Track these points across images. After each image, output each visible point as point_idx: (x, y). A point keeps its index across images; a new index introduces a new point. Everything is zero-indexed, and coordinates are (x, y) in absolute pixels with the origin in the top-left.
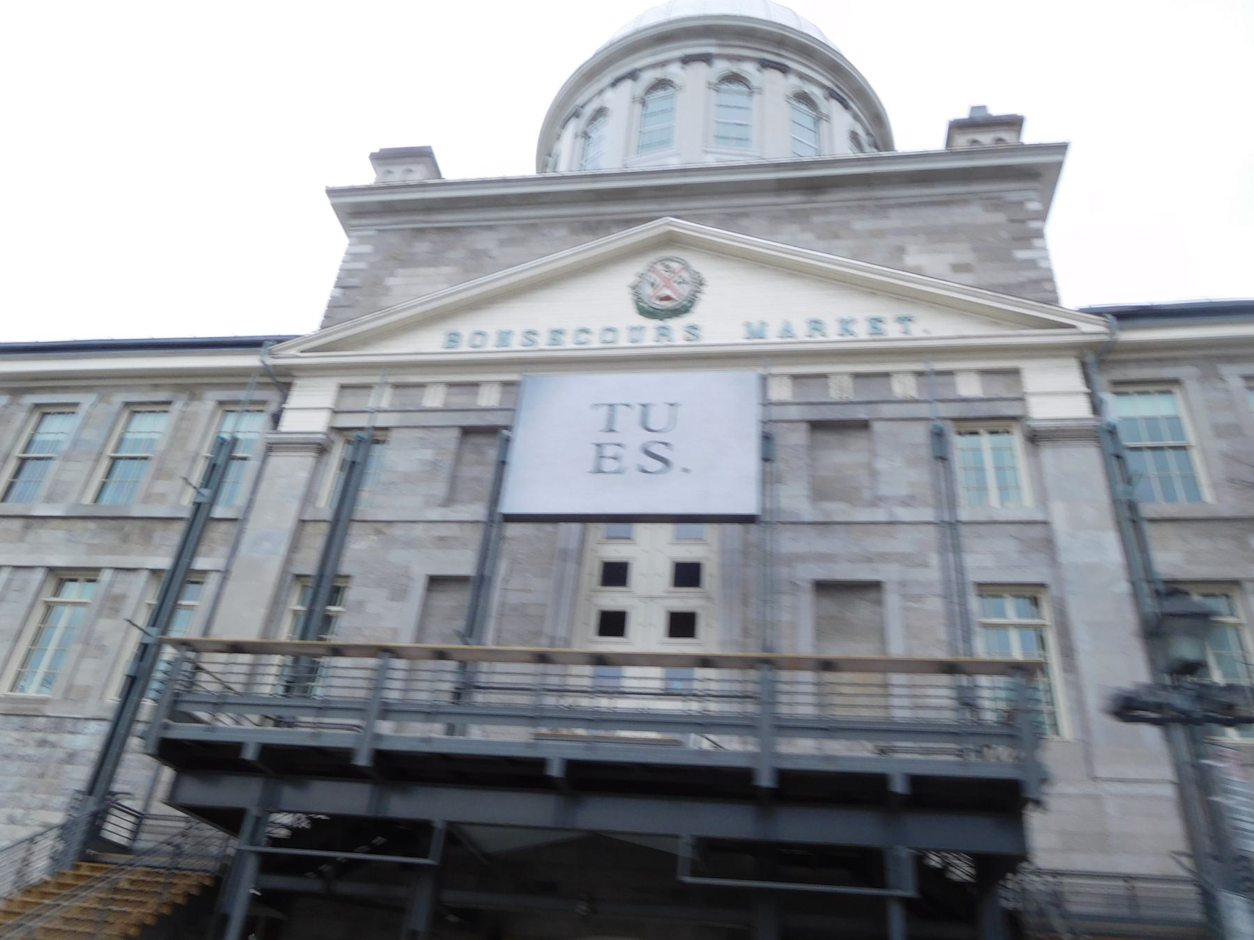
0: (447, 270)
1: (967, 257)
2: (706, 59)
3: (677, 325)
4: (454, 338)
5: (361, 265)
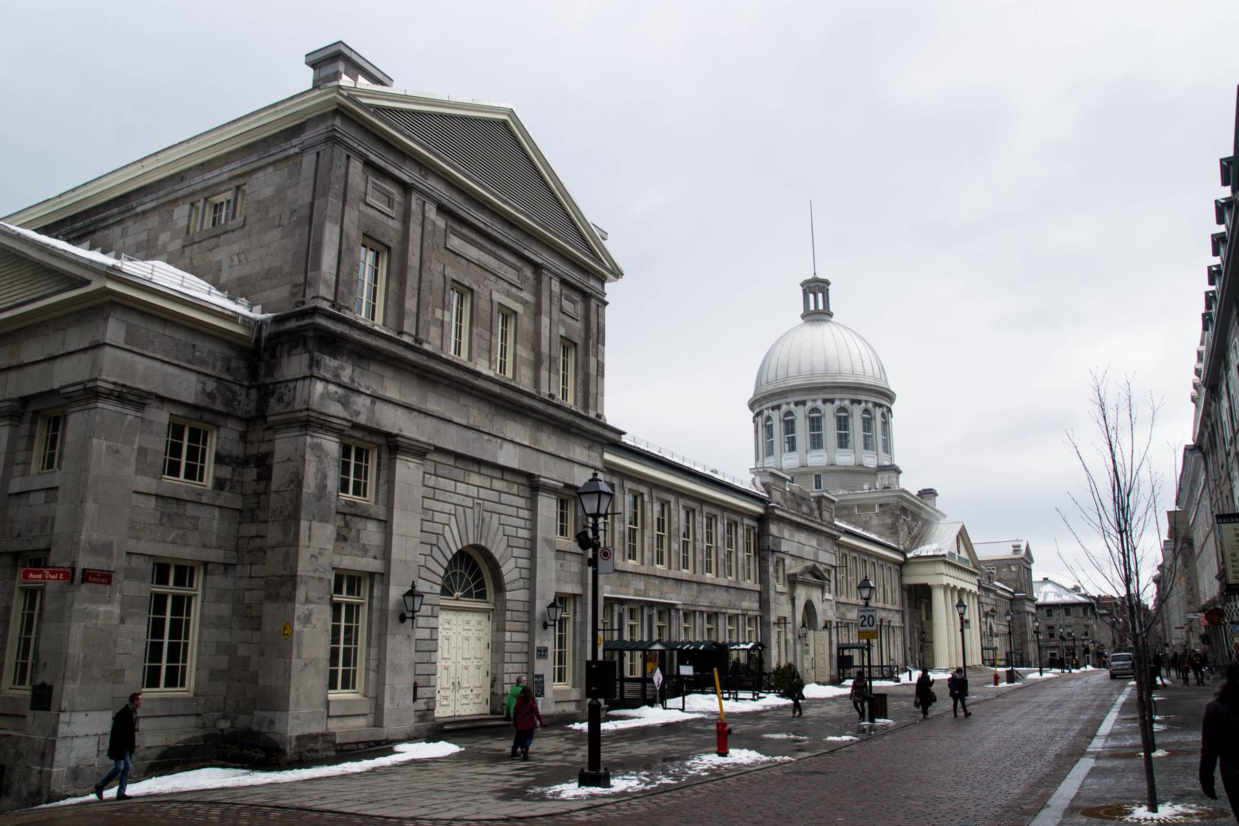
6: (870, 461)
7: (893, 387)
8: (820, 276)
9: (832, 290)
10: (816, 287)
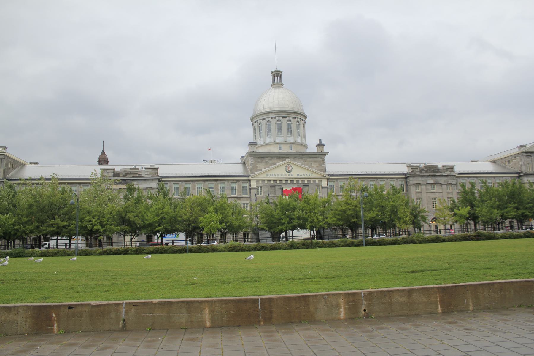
0: (263, 164)
1: (318, 165)
2: (286, 117)
3: (290, 173)
4: (267, 175)
5: (253, 163)
6: (299, 141)
7: (306, 113)
8: (278, 70)
9: (283, 75)
10: (277, 74)
